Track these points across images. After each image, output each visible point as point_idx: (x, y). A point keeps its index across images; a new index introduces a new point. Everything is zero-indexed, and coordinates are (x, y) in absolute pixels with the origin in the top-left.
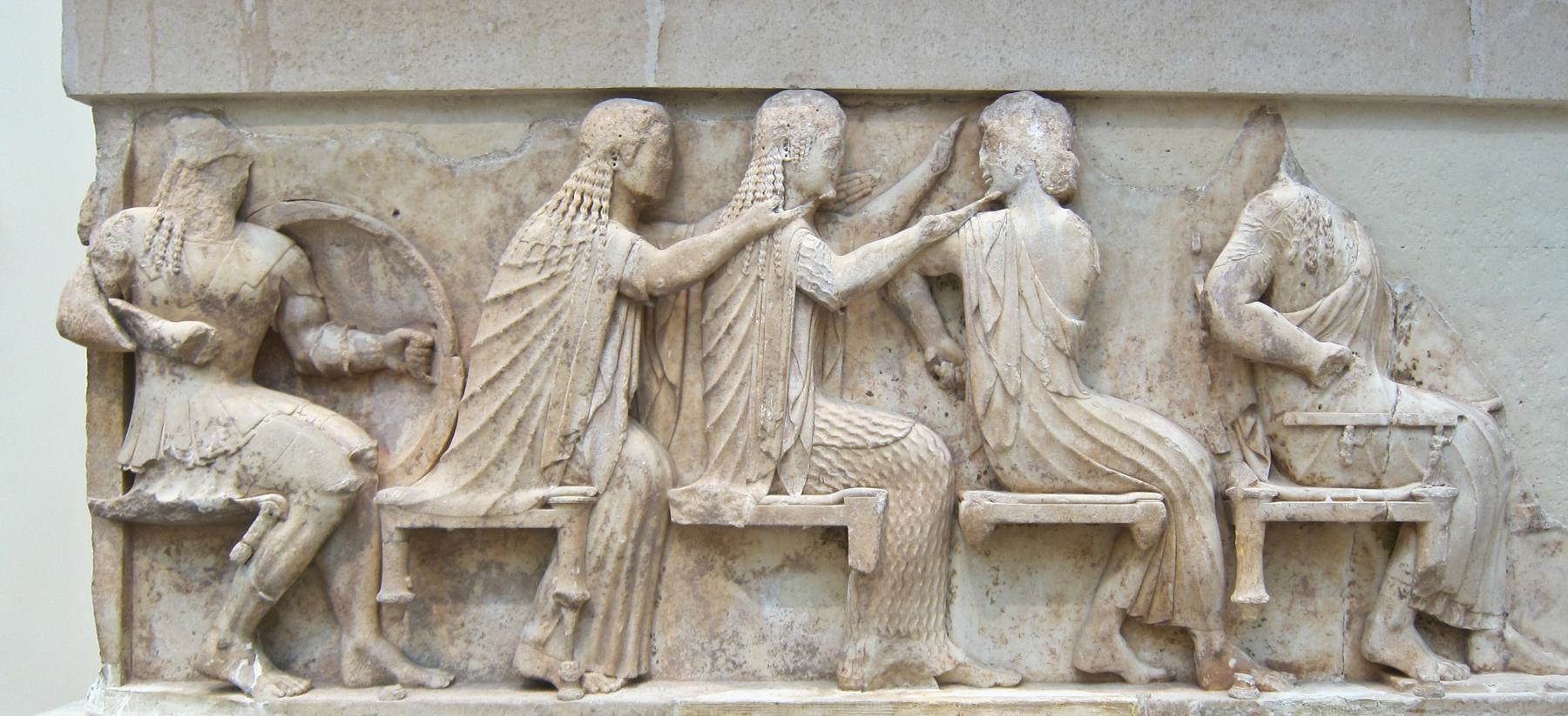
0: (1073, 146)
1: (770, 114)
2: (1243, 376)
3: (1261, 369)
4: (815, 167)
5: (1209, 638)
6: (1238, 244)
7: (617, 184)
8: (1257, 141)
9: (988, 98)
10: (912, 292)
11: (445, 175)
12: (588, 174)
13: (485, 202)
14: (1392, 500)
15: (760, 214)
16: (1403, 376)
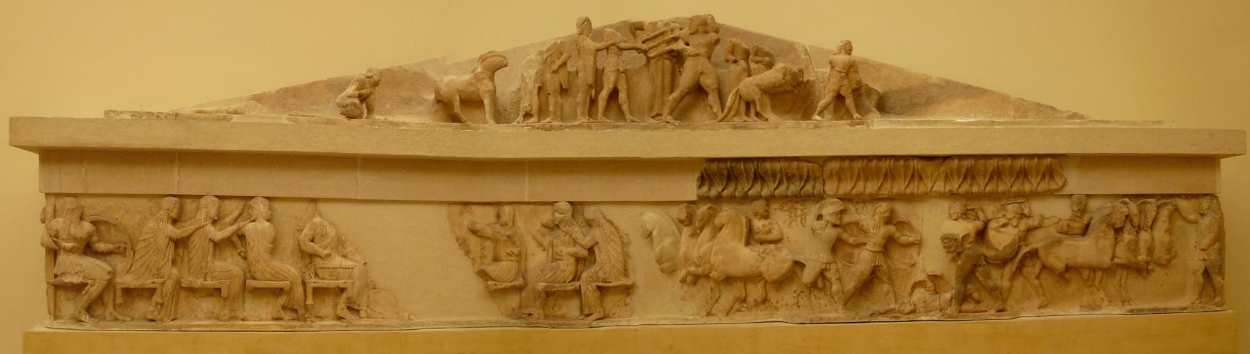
0: (270, 209)
1: (203, 201)
2: (309, 257)
3: (313, 256)
4: (213, 213)
5: (302, 311)
6: (306, 231)
7: (169, 216)
8: (311, 206)
9: (252, 197)
10: (235, 239)
11: (128, 211)
12: (162, 214)
13: (137, 217)
14: (341, 283)
15: (202, 222)
16: (345, 256)
